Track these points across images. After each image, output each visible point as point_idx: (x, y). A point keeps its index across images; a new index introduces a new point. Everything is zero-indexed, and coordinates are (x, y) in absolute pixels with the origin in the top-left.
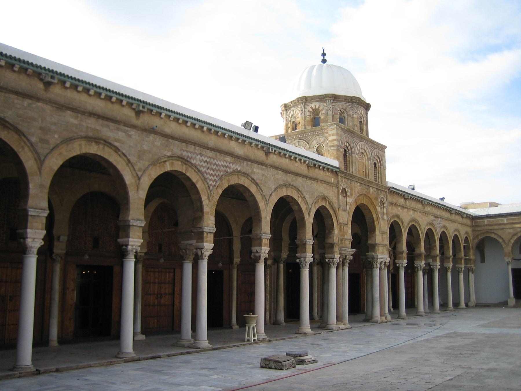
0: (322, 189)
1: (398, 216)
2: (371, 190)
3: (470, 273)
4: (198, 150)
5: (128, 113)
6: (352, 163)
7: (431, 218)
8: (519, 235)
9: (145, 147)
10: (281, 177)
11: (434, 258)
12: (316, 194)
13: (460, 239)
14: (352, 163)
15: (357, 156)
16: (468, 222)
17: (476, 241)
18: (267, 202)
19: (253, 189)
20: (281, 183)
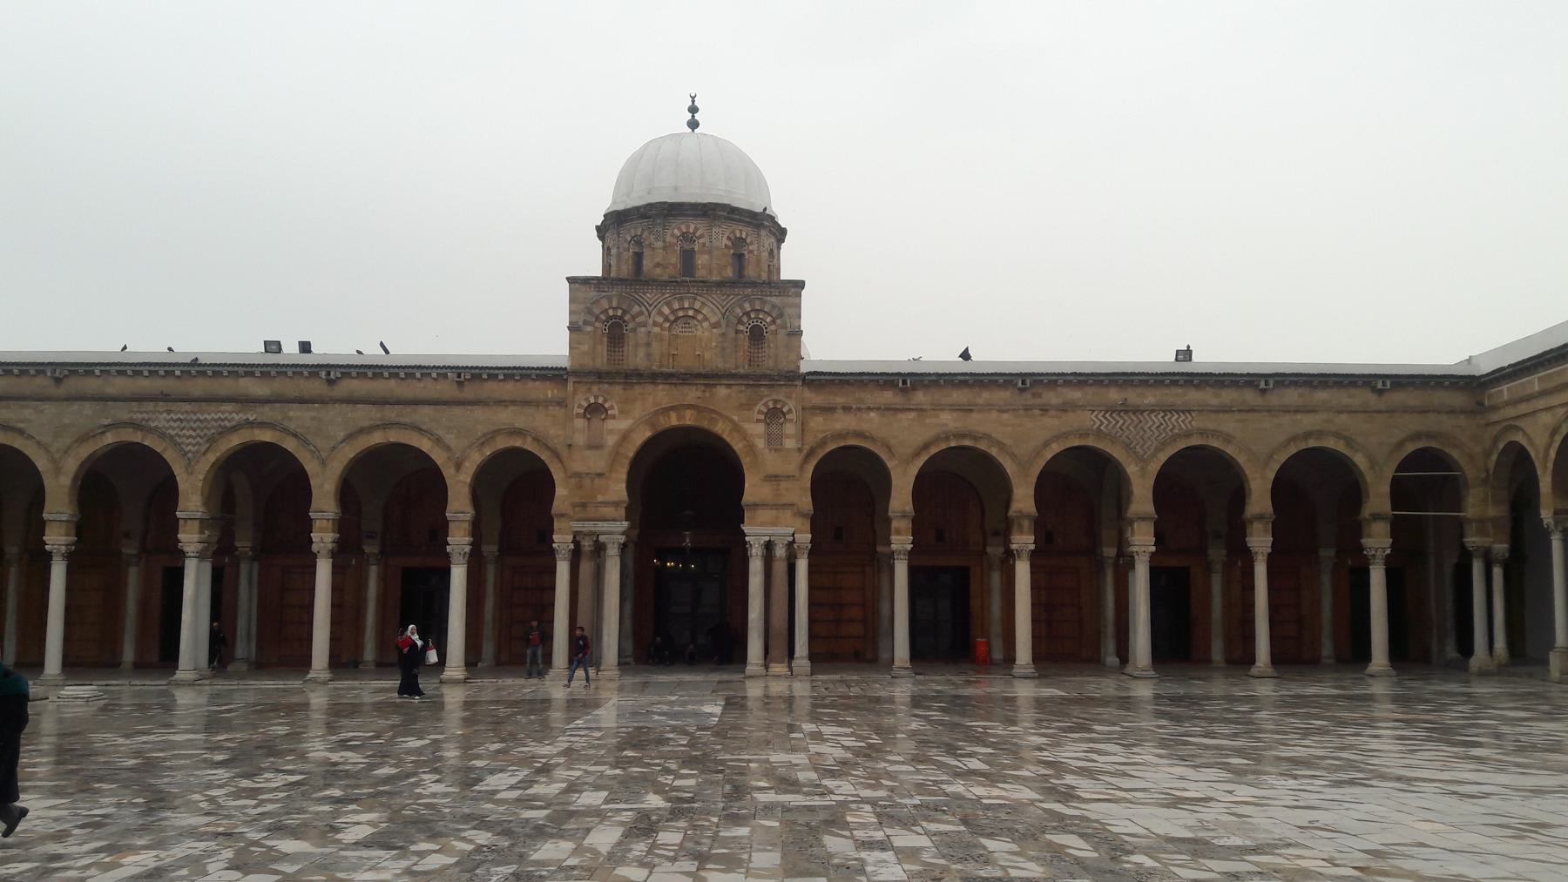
0: (505, 416)
1: (860, 435)
2: (722, 391)
3: (1477, 568)
4: (162, 406)
5: (42, 383)
6: (637, 345)
7: (1089, 419)
8: (1564, 431)
9: (66, 421)
10: (364, 415)
11: (1131, 522)
12: (481, 429)
13: (1360, 460)
14: (637, 345)
15: (657, 330)
16: (1458, 399)
17: (1494, 457)
18: (323, 463)
19: (290, 445)
20: (366, 424)
